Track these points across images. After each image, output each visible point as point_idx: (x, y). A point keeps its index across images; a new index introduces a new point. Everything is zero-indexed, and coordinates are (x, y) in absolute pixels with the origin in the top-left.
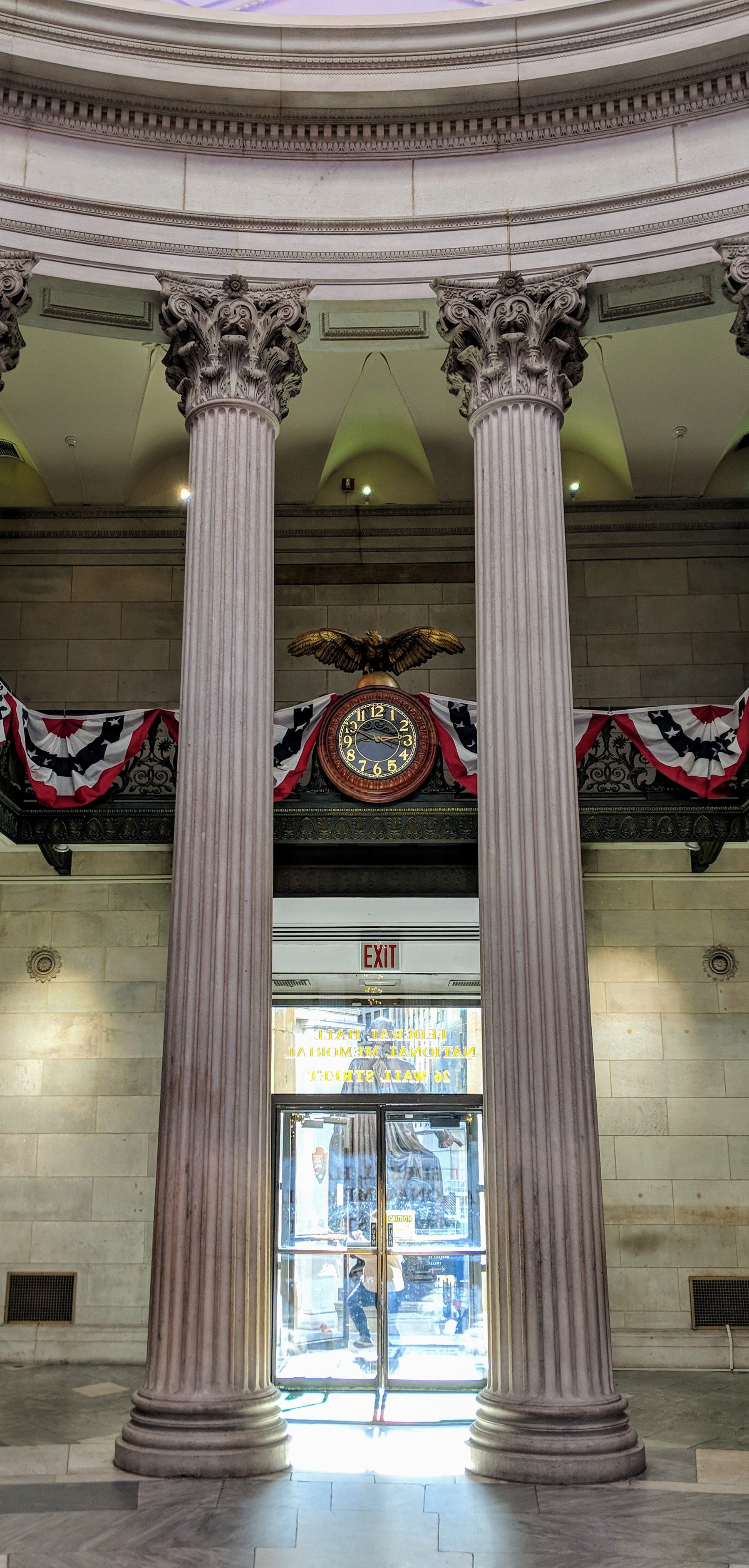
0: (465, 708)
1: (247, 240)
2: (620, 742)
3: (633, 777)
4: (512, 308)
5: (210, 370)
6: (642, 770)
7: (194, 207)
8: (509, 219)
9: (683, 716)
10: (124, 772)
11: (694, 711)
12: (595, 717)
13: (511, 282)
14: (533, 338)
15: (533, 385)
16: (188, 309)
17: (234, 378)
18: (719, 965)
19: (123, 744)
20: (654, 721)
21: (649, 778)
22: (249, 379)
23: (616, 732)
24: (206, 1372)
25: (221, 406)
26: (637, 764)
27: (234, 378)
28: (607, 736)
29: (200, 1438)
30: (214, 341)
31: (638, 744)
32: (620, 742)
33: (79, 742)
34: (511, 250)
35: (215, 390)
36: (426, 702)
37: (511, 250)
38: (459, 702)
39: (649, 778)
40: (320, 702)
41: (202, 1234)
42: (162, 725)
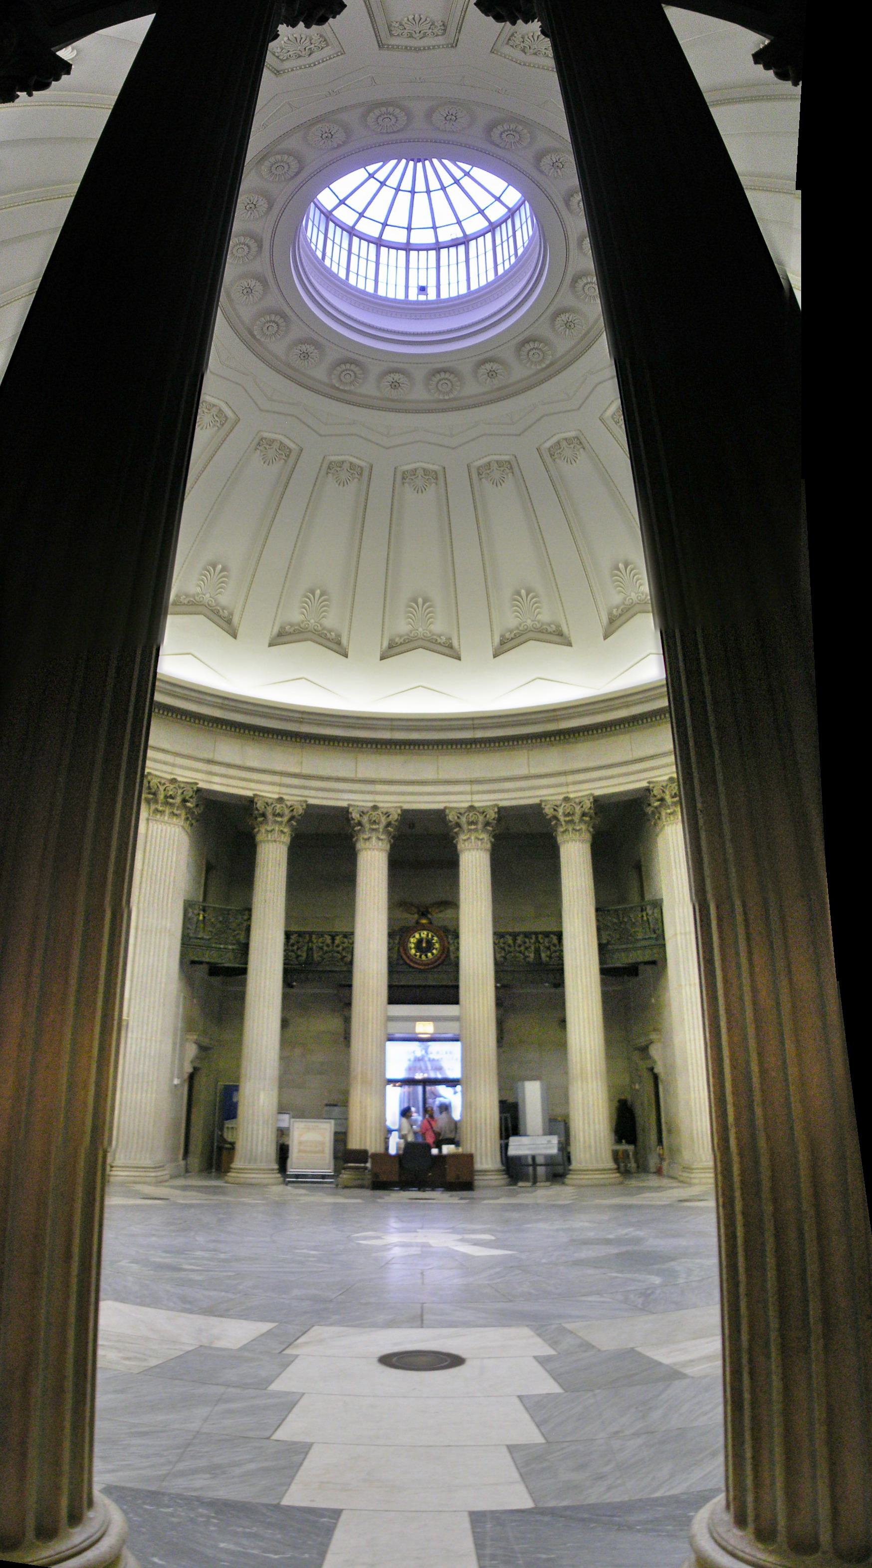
1: (379, 787)
4: (472, 816)
5: (366, 837)
7: (360, 775)
8: (471, 782)
13: (472, 808)
14: (480, 826)
15: (480, 843)
16: (358, 816)
17: (374, 839)
22: (379, 839)
25: (370, 849)
27: (374, 839)
30: (367, 826)
35: (367, 843)
37: (472, 793)
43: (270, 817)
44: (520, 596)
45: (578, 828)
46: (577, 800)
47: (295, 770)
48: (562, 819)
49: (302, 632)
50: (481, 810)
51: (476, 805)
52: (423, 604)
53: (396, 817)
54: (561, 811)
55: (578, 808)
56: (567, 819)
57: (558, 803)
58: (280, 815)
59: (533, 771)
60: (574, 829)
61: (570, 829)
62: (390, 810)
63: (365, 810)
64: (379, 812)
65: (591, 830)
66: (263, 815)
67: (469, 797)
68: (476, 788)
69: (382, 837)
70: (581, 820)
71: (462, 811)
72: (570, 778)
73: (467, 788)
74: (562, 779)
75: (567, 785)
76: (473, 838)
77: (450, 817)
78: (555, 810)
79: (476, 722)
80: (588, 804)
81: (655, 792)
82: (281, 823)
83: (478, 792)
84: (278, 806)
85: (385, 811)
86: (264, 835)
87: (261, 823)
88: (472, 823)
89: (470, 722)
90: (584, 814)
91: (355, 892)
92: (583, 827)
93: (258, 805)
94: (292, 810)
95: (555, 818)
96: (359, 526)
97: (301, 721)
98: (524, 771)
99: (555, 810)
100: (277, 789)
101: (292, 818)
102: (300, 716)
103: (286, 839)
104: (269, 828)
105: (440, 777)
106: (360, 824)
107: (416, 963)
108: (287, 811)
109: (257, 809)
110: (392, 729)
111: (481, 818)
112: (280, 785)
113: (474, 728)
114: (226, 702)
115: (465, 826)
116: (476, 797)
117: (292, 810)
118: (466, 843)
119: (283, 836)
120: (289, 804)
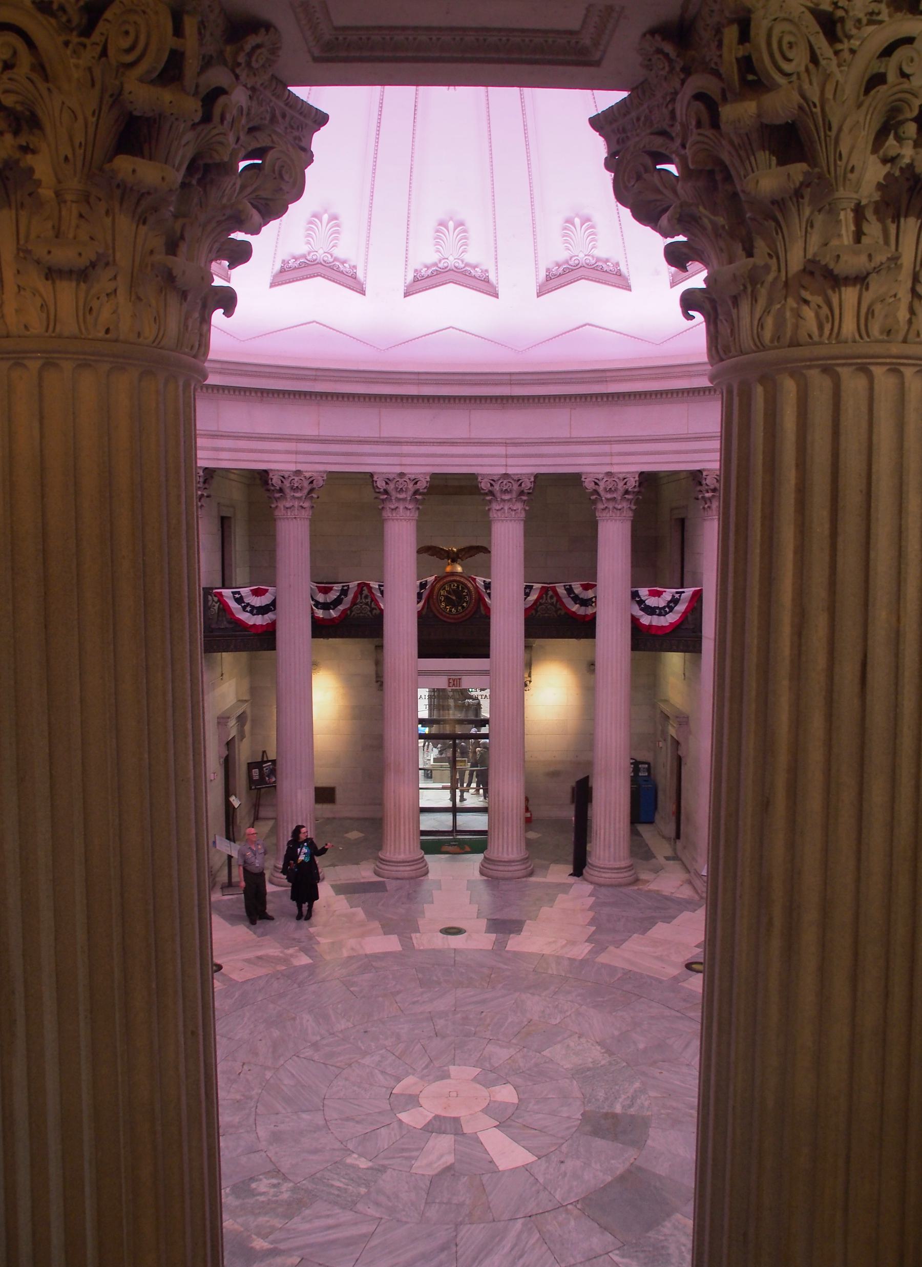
0: (490, 583)
1: (406, 449)
2: (551, 597)
3: (556, 612)
5: (393, 507)
6: (560, 609)
9: (578, 590)
10: (350, 608)
11: (582, 585)
12: (543, 587)
13: (506, 476)
14: (514, 495)
18: (592, 667)
19: (351, 596)
20: (566, 589)
21: (563, 612)
23: (550, 593)
24: (402, 850)
26: (558, 606)
28: (547, 594)
29: (401, 868)
30: (394, 494)
31: (559, 599)
32: (551, 597)
33: (333, 596)
34: (506, 456)
36: (474, 580)
37: (506, 456)
38: (488, 580)
39: (563, 612)
40: (431, 579)
41: (400, 812)
42: (365, 588)
43: (287, 491)
44: (573, 225)
45: (619, 507)
46: (621, 476)
47: (311, 432)
48: (602, 493)
49: (309, 265)
50: (516, 478)
51: (510, 471)
52: (455, 230)
53: (425, 485)
54: (602, 484)
55: (621, 484)
56: (609, 496)
57: (600, 477)
58: (297, 489)
59: (577, 433)
60: (614, 508)
61: (611, 507)
62: (419, 477)
63: (391, 477)
64: (406, 479)
65: (634, 507)
66: (281, 490)
67: (503, 461)
68: (512, 450)
69: (410, 507)
70: (623, 498)
71: (496, 478)
72: (617, 448)
73: (501, 450)
74: (606, 448)
75: (611, 455)
76: (506, 508)
77: (483, 485)
78: (596, 484)
79: (514, 377)
80: (632, 482)
81: (708, 482)
82: (299, 498)
83: (513, 456)
84: (296, 479)
85: (413, 477)
86: (283, 511)
87: (277, 499)
88: (506, 492)
89: (508, 377)
90: (627, 492)
91: (382, 551)
92: (625, 505)
93: (274, 482)
94: (312, 482)
95: (596, 492)
96: (375, 121)
97: (315, 379)
98: (564, 433)
99: (596, 484)
100: (292, 457)
101: (311, 491)
102: (314, 373)
103: (305, 514)
104: (288, 505)
105: (473, 436)
106: (386, 492)
107: (445, 616)
108: (306, 484)
109: (273, 485)
110: (420, 383)
111: (515, 487)
112: (297, 453)
113: (511, 383)
114: (225, 366)
115: (498, 495)
116: (511, 461)
117: (312, 482)
118: (499, 513)
119: (303, 511)
120: (308, 475)
